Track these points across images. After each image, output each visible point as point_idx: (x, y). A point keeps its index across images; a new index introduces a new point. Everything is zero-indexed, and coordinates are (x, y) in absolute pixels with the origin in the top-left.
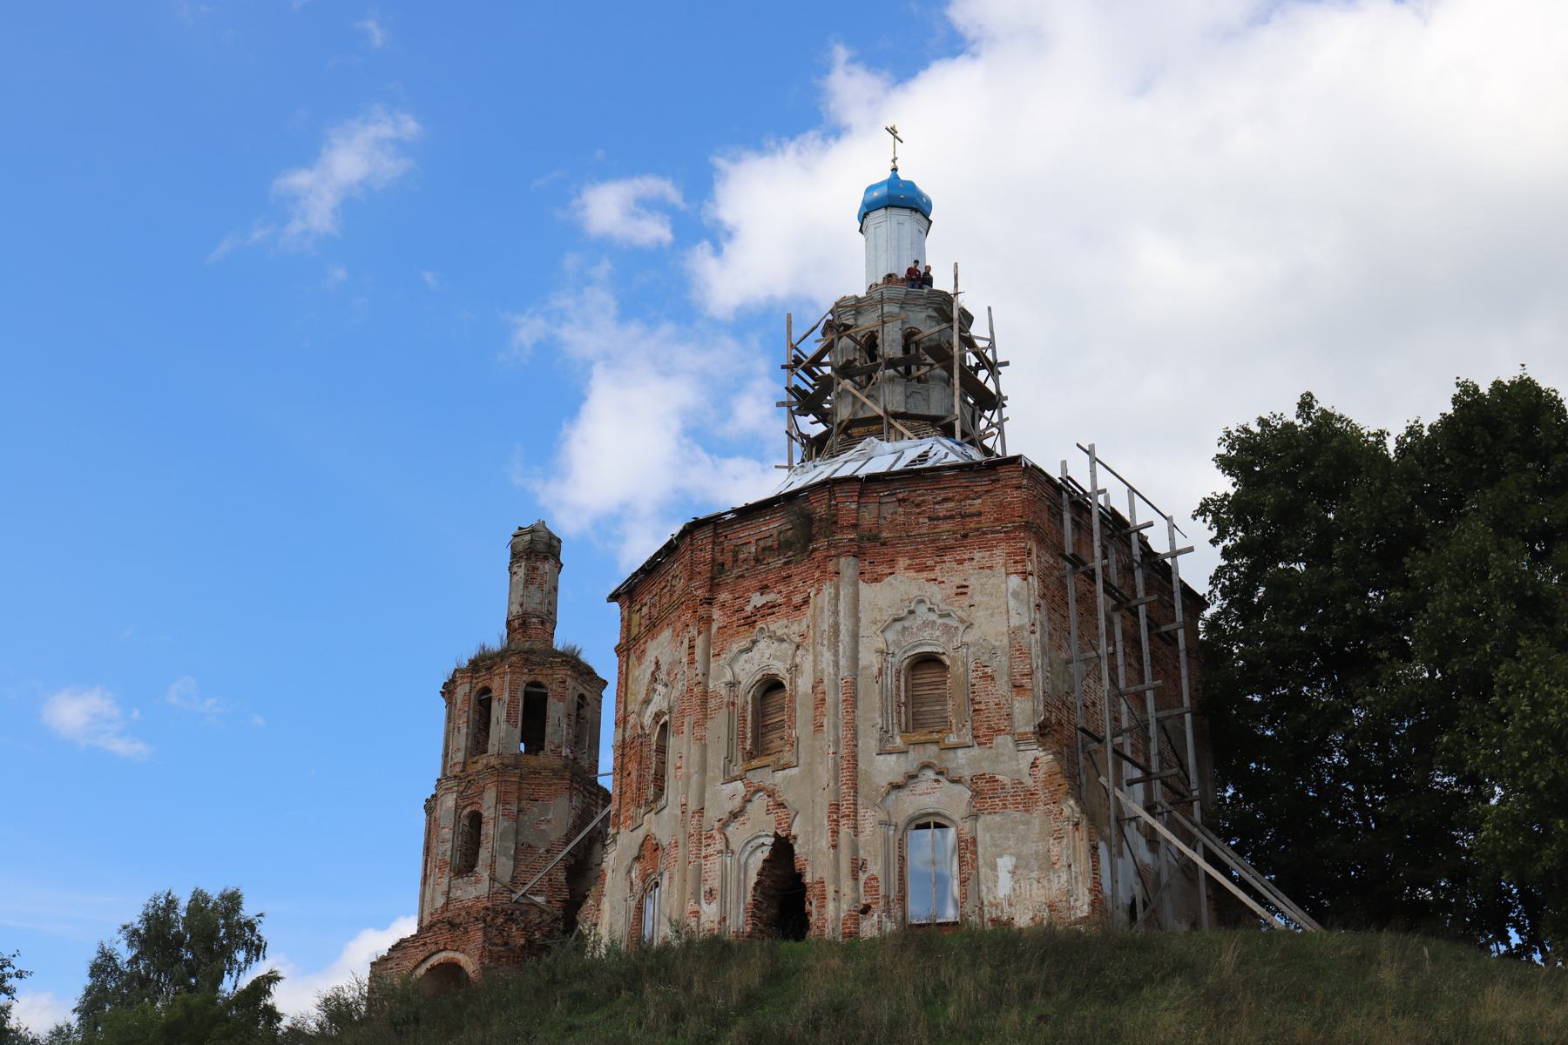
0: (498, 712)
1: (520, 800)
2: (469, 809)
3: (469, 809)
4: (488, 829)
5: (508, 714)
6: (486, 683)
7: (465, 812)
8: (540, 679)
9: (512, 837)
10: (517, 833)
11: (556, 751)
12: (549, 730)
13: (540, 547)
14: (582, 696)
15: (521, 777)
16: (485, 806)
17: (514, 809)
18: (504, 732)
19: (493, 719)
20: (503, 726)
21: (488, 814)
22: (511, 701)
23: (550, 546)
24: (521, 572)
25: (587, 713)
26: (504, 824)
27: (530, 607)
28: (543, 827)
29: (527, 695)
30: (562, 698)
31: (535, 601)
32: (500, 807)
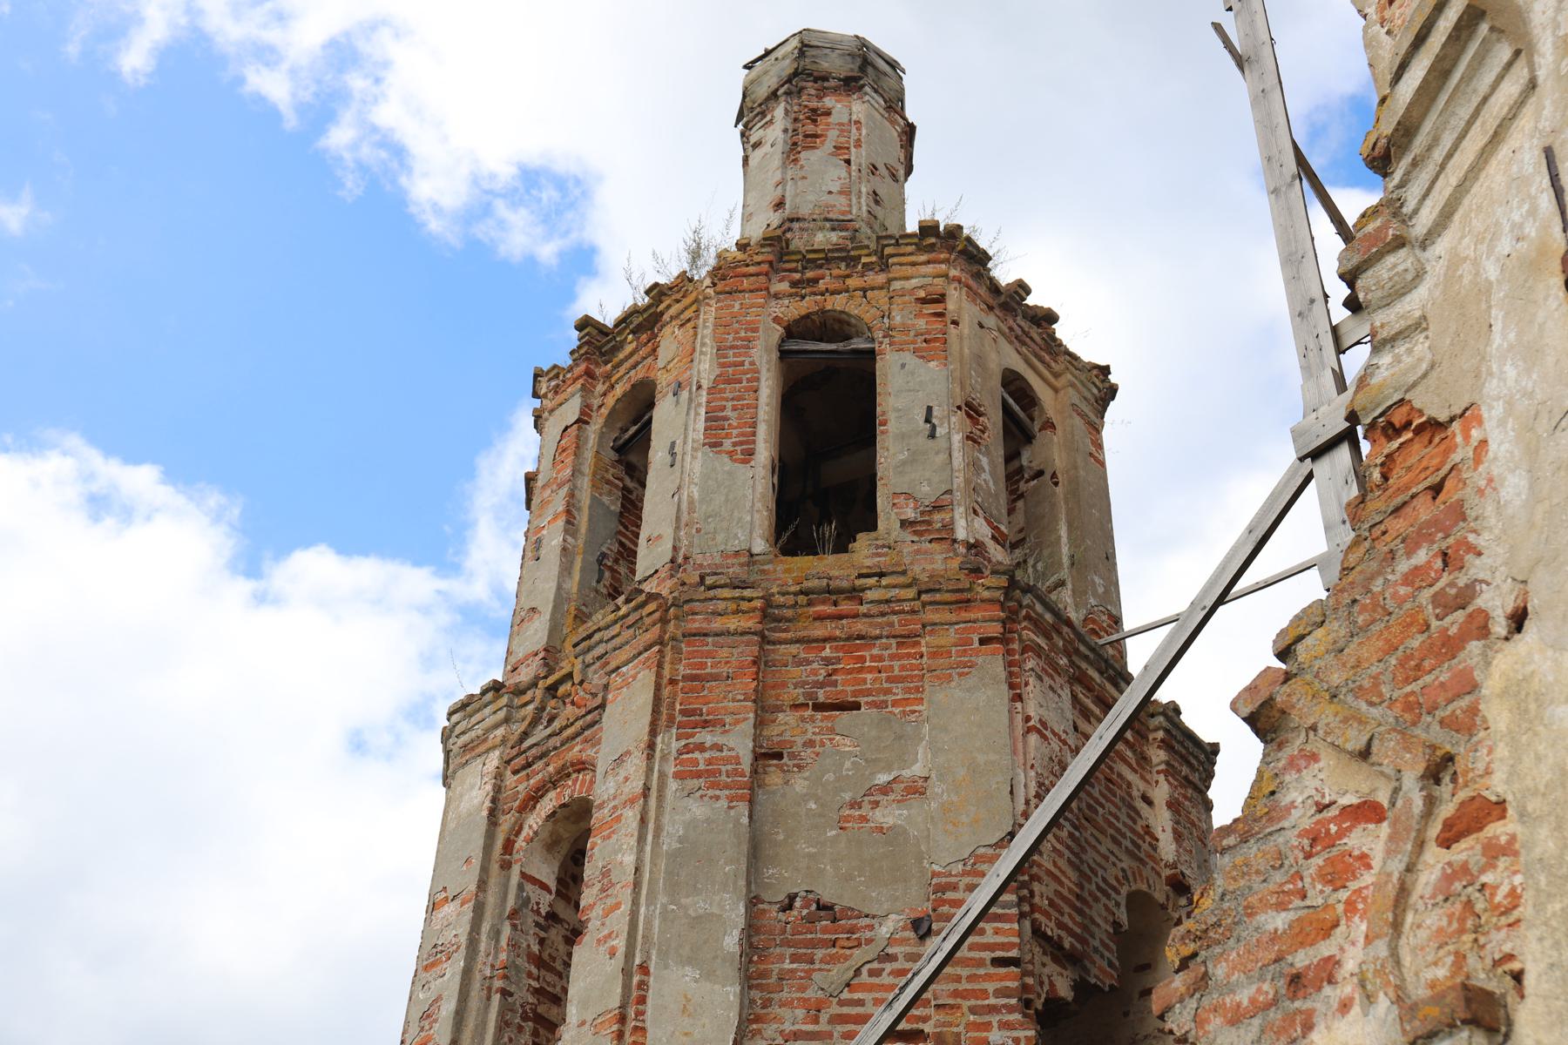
0: (673, 423)
1: (764, 712)
2: (548, 804)
3: (548, 804)
4: (613, 853)
5: (715, 420)
6: (638, 374)
7: (534, 821)
8: (837, 303)
9: (731, 865)
10: (756, 852)
11: (928, 523)
12: (890, 454)
13: (836, 65)
14: (1012, 381)
15: (765, 615)
16: (603, 757)
17: (739, 742)
18: (711, 490)
19: (658, 455)
20: (696, 463)
21: (614, 783)
22: (723, 380)
23: (866, 63)
24: (775, 132)
25: (1051, 451)
26: (691, 811)
27: (805, 201)
28: (888, 815)
29: (784, 354)
30: (932, 346)
31: (824, 183)
32: (669, 742)
